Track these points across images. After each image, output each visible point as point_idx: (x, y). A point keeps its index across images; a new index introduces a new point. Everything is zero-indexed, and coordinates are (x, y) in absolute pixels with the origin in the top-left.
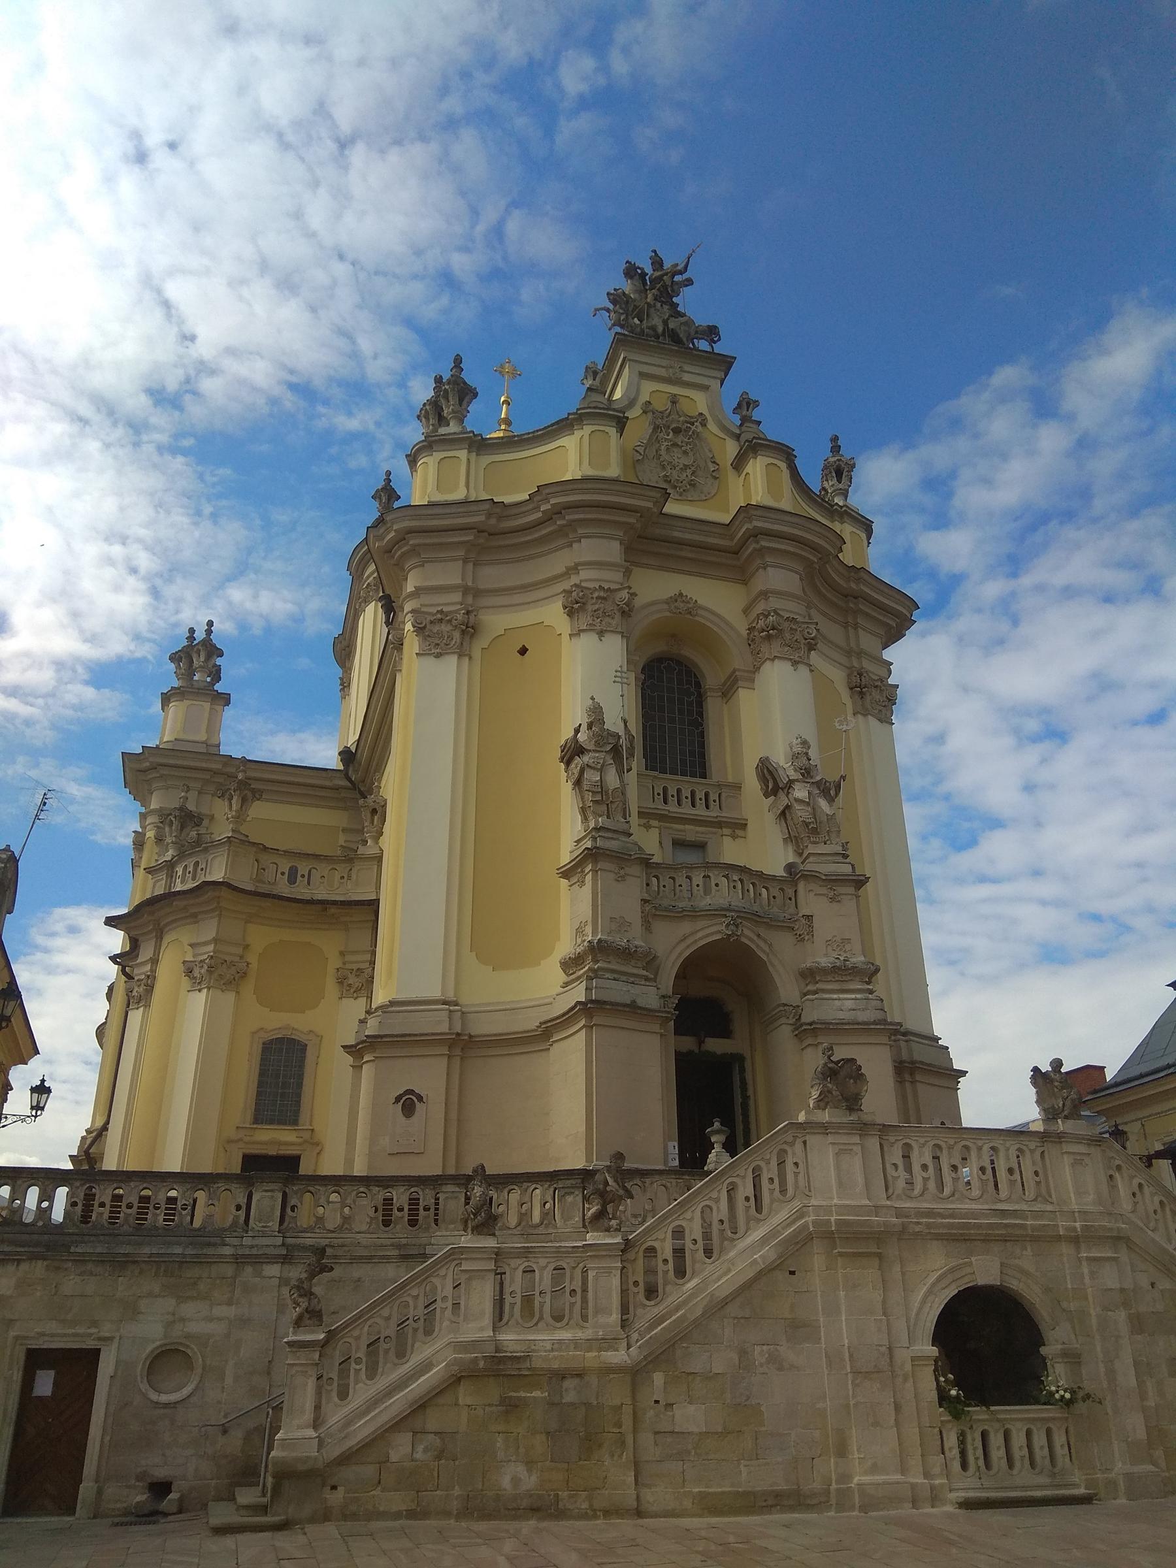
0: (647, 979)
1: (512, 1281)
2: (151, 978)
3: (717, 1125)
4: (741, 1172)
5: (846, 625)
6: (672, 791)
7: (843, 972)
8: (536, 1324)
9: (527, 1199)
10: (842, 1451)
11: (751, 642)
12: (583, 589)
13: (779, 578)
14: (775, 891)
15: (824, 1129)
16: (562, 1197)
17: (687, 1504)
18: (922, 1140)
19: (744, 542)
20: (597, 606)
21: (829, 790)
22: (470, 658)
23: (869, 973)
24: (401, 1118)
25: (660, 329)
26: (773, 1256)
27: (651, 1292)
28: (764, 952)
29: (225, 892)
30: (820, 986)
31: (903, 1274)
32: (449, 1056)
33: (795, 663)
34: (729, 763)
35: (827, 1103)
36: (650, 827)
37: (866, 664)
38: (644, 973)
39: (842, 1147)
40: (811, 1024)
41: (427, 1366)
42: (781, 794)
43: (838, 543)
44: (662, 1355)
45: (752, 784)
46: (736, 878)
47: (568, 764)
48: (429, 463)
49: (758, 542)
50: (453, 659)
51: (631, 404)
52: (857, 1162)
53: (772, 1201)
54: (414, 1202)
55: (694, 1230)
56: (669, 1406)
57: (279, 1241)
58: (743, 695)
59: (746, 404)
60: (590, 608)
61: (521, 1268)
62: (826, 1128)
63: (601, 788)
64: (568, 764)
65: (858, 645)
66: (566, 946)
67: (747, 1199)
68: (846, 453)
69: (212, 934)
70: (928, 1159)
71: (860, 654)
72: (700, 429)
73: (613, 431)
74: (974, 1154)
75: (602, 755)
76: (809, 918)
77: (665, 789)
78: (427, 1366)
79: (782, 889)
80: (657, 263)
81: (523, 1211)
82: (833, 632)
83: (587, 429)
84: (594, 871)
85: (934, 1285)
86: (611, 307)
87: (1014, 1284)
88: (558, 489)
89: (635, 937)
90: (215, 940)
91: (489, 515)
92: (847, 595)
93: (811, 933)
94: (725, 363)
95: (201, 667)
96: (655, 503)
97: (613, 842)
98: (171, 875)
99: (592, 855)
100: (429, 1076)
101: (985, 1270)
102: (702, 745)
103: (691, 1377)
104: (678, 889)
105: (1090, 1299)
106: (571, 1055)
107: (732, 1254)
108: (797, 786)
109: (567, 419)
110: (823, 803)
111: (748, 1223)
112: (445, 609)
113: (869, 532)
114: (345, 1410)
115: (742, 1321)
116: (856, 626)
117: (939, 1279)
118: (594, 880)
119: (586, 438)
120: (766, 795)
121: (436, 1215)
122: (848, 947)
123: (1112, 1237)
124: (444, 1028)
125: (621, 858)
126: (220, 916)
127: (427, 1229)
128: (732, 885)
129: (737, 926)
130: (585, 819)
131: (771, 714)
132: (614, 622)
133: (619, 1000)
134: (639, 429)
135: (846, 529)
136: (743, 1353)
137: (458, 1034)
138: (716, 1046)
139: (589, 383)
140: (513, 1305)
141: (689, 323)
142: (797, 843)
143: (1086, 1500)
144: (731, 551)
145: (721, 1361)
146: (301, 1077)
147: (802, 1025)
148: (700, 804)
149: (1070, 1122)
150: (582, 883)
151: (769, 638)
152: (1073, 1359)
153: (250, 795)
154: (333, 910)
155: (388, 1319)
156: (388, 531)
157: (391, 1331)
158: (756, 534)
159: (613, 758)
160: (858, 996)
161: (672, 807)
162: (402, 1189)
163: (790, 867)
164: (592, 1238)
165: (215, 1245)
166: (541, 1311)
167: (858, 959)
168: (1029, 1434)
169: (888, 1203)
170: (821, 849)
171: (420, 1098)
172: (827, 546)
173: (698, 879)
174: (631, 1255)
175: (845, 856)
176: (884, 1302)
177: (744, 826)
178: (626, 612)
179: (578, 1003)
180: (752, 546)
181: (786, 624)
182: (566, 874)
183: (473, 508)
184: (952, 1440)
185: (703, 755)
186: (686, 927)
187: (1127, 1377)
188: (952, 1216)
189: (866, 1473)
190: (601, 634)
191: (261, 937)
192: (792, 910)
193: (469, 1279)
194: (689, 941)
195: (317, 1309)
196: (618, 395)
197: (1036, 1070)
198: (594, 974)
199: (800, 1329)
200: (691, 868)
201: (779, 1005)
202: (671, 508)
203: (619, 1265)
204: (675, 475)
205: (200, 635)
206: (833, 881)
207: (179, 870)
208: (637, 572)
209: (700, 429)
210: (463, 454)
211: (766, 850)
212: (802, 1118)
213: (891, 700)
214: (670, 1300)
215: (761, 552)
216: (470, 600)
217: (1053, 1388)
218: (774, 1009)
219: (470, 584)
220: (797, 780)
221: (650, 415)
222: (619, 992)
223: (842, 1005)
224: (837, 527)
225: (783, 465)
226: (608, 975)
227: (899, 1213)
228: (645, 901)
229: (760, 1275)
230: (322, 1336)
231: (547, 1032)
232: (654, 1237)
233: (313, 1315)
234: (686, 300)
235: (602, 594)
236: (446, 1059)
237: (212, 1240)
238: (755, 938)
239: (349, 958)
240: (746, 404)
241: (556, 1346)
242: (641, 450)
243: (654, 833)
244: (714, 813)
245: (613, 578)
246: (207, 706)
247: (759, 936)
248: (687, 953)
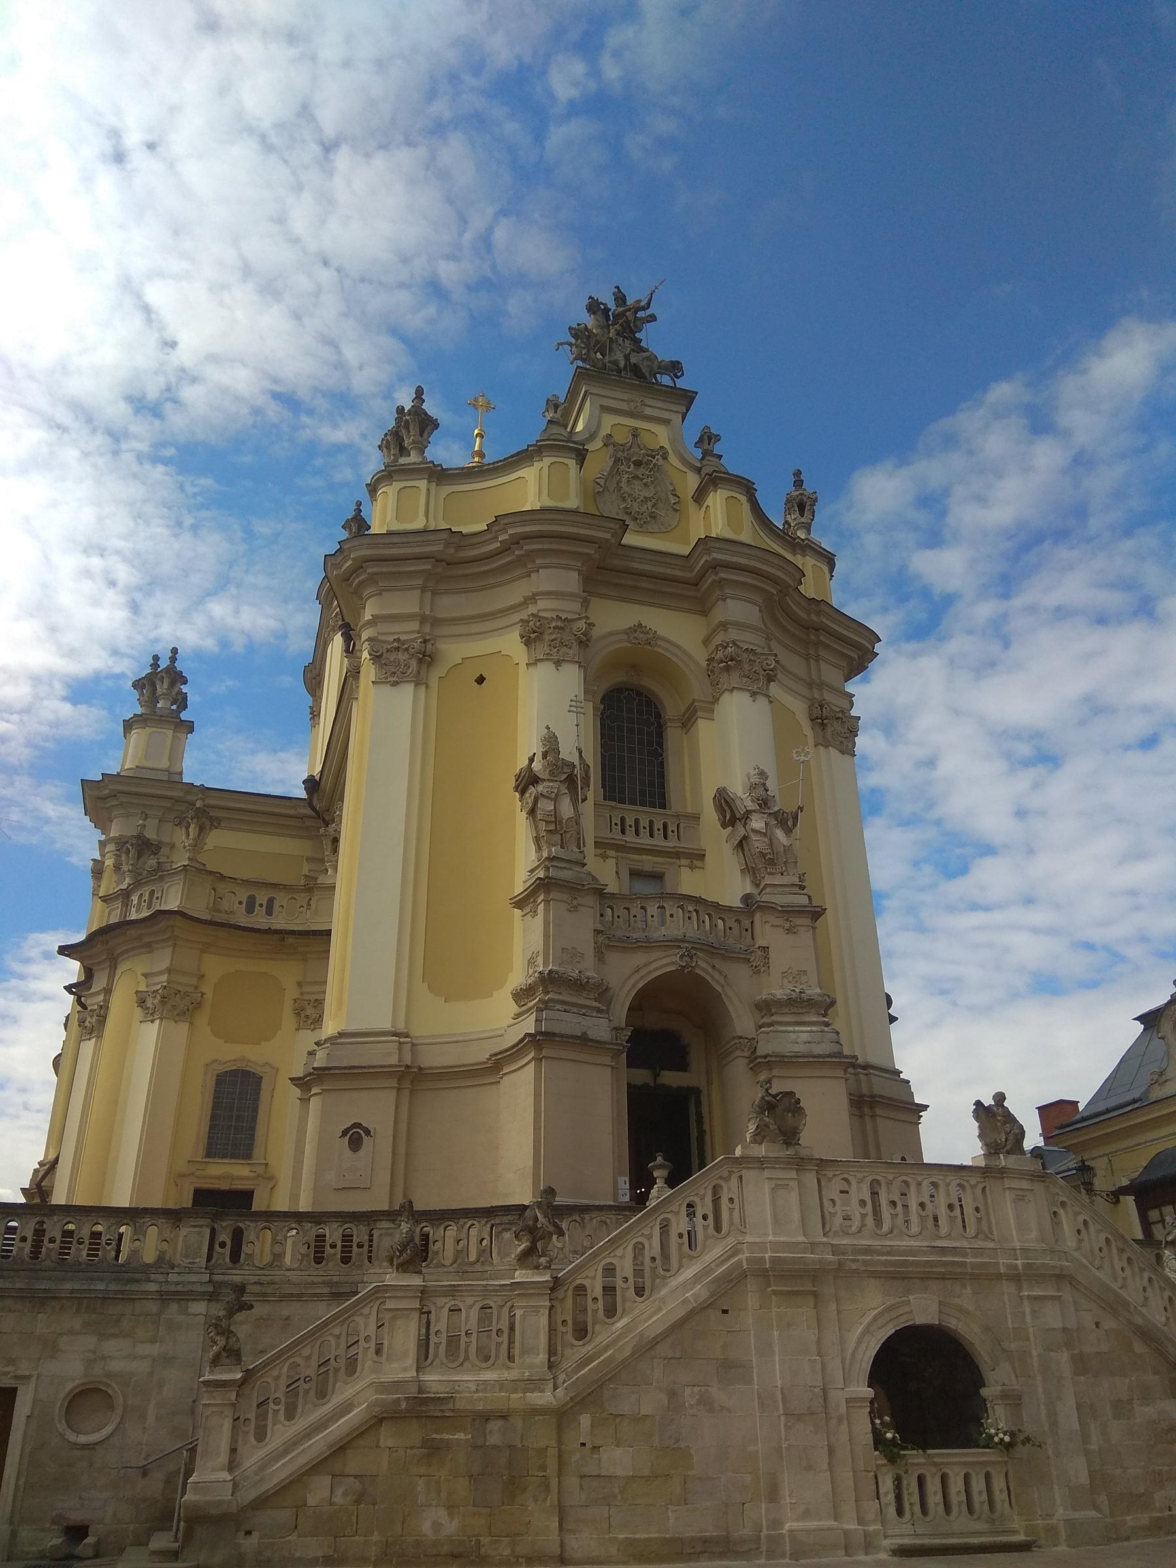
0: (599, 1010)
1: (438, 1320)
2: (104, 1008)
3: (660, 1160)
4: (675, 1208)
5: (807, 657)
6: (630, 821)
7: (798, 1004)
8: (461, 1365)
9: (463, 1235)
10: (773, 1495)
11: (710, 672)
12: (540, 618)
13: (738, 609)
14: (731, 923)
15: (760, 1163)
16: (499, 1234)
17: (613, 1551)
18: (860, 1176)
19: (703, 575)
20: (553, 637)
21: (787, 821)
22: (427, 687)
23: (826, 1006)
24: (348, 1152)
25: (622, 363)
26: (705, 1294)
27: (581, 1332)
28: (719, 983)
29: (179, 921)
31: (839, 1312)
32: (398, 1089)
33: (754, 694)
34: (688, 795)
35: (764, 1137)
37: (829, 697)
38: (596, 1004)
39: (779, 1182)
40: (765, 1057)
41: (347, 1407)
42: (739, 824)
43: (798, 576)
44: (589, 1397)
45: (710, 814)
46: (691, 909)
47: (523, 793)
48: (389, 493)
49: (717, 574)
50: (411, 687)
51: (592, 437)
52: (794, 1197)
53: (706, 1238)
54: (347, 1238)
55: (625, 1266)
56: (596, 1448)
57: (206, 1278)
58: (703, 726)
59: (707, 438)
60: (547, 637)
61: (448, 1306)
62: (762, 1163)
63: (555, 818)
64: (523, 793)
65: (820, 676)
66: (518, 977)
67: (681, 1236)
68: (808, 487)
69: (165, 964)
70: (866, 1195)
71: (821, 685)
72: (661, 462)
73: (572, 463)
74: (913, 1188)
75: (556, 785)
76: (765, 949)
77: (623, 820)
78: (347, 1407)
79: (738, 921)
80: (620, 298)
81: (459, 1248)
82: (793, 662)
83: (547, 461)
84: (547, 902)
85: (869, 1325)
86: (573, 341)
87: (954, 1323)
88: (517, 519)
89: (588, 968)
90: (169, 971)
91: (447, 545)
92: (808, 627)
93: (767, 964)
94: (687, 398)
95: (163, 694)
96: (614, 534)
97: (566, 872)
98: (126, 904)
99: (543, 885)
100: (376, 1109)
101: (923, 1310)
102: (662, 775)
103: (618, 1419)
104: (632, 919)
105: (1032, 1339)
106: (520, 1087)
107: (663, 1293)
108: (754, 817)
109: (527, 450)
110: (780, 834)
111: (680, 1261)
112: (403, 637)
113: (832, 566)
114: (261, 1453)
115: (673, 1361)
116: (817, 659)
117: (875, 1319)
118: (546, 910)
119: (546, 470)
120: (724, 826)
121: (370, 1252)
123: (1055, 1275)
124: (394, 1060)
125: (573, 888)
126: (175, 946)
127: (360, 1267)
128: (687, 915)
129: (691, 958)
130: (539, 849)
131: (730, 745)
132: (571, 652)
133: (568, 1032)
134: (599, 462)
135: (807, 563)
136: (672, 1394)
137: (407, 1067)
138: (672, 1078)
139: (549, 416)
140: (437, 1345)
141: (652, 358)
142: (754, 874)
143: (1025, 1547)
144: (691, 582)
145: (650, 1403)
146: (255, 1110)
147: (756, 1058)
148: (658, 834)
149: (1013, 1158)
150: (535, 913)
151: (728, 669)
152: (1014, 1400)
153: (208, 823)
154: (291, 940)
155: (309, 1358)
156: (345, 559)
157: (311, 1371)
158: (715, 566)
159: (568, 788)
160: (814, 1029)
161: (630, 838)
162: (335, 1225)
163: (747, 898)
164: (521, 1276)
165: (137, 1281)
166: (466, 1351)
167: (814, 991)
168: (967, 1477)
169: (825, 1239)
170: (778, 880)
171: (368, 1132)
172: (787, 579)
173: (652, 909)
174: (560, 1294)
175: (802, 888)
176: (819, 1342)
177: (701, 857)
178: (584, 642)
179: (527, 1035)
180: (710, 579)
181: (745, 655)
182: (520, 903)
183: (431, 537)
184: (887, 1484)
185: (662, 785)
186: (640, 958)
187: (1069, 1419)
188: (889, 1253)
189: (797, 1520)
190: (558, 663)
191: (216, 967)
192: (749, 941)
193: (393, 1318)
194: (643, 972)
195: (236, 1347)
196: (580, 427)
197: (978, 1104)
198: (545, 1006)
199: (731, 1369)
200: (647, 898)
201: (734, 1038)
202: (629, 539)
203: (547, 1303)
204: (636, 507)
205: (164, 664)
206: (789, 912)
207: (135, 899)
208: (595, 602)
209: (661, 462)
210: (422, 484)
211: (723, 880)
212: (738, 1152)
213: (853, 732)
214: (599, 1340)
215: (721, 583)
216: (427, 629)
217: (993, 1431)
218: (728, 1042)
219: (427, 612)
220: (754, 811)
221: (611, 448)
222: (570, 1024)
223: (798, 1037)
224: (798, 560)
225: (743, 499)
226: (558, 1007)
227: (836, 1250)
228: (598, 932)
229: (692, 1314)
230: (239, 1376)
231: (497, 1065)
232: (583, 1275)
233: (233, 1354)
234: (649, 336)
235: (559, 624)
236: (394, 1092)
237: (137, 1276)
238: (710, 970)
239: (306, 989)
240: (707, 438)
241: (480, 1388)
242: (602, 482)
243: (611, 863)
244: (672, 843)
245: (570, 608)
246: (170, 733)
247: (714, 967)
248: (640, 986)
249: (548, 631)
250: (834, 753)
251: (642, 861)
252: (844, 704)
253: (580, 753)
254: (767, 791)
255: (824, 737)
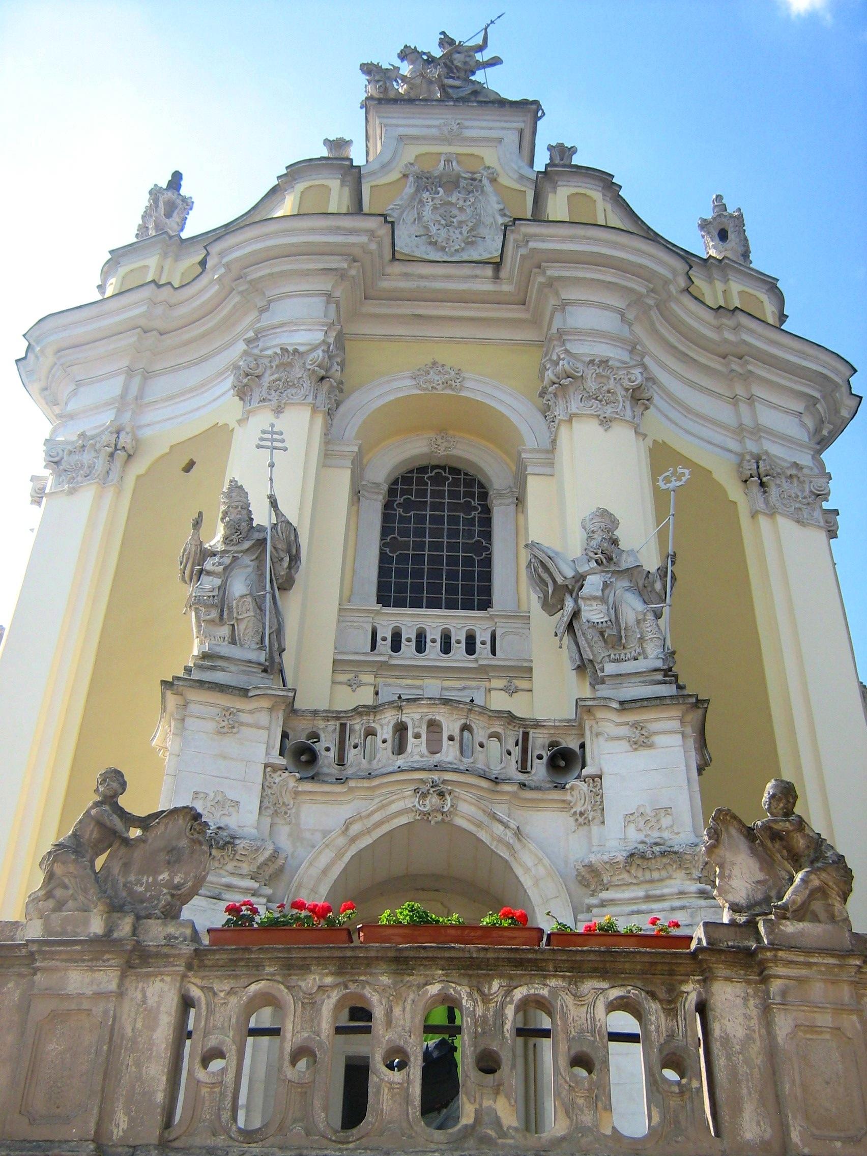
6: (408, 633)
20: (276, 376)
30: (605, 895)
33: (606, 422)
36: (360, 685)
49: (544, 273)
58: (534, 486)
60: (267, 379)
68: (730, 209)
71: (758, 431)
73: (334, 184)
83: (300, 187)
102: (487, 577)
122: (666, 821)
177: (527, 671)
178: (331, 382)
225: (597, 195)
235: (285, 360)
249: (269, 372)
250: (785, 524)
251: (419, 687)
252: (805, 459)
253: (274, 504)
254: (615, 542)
255: (767, 503)
